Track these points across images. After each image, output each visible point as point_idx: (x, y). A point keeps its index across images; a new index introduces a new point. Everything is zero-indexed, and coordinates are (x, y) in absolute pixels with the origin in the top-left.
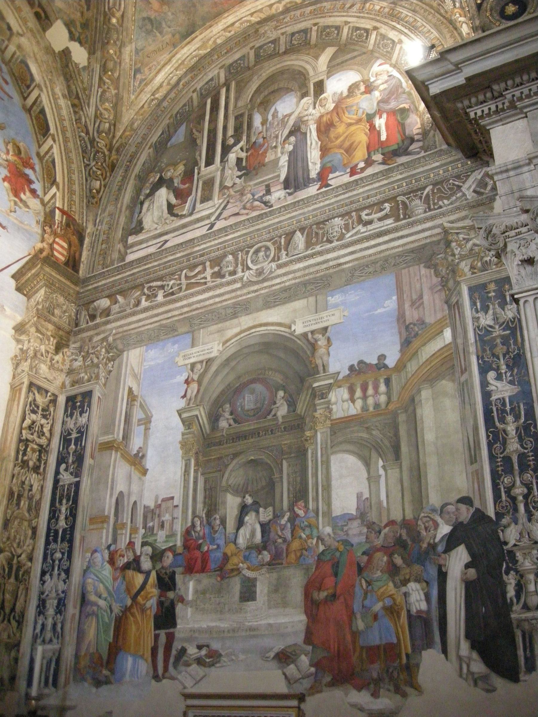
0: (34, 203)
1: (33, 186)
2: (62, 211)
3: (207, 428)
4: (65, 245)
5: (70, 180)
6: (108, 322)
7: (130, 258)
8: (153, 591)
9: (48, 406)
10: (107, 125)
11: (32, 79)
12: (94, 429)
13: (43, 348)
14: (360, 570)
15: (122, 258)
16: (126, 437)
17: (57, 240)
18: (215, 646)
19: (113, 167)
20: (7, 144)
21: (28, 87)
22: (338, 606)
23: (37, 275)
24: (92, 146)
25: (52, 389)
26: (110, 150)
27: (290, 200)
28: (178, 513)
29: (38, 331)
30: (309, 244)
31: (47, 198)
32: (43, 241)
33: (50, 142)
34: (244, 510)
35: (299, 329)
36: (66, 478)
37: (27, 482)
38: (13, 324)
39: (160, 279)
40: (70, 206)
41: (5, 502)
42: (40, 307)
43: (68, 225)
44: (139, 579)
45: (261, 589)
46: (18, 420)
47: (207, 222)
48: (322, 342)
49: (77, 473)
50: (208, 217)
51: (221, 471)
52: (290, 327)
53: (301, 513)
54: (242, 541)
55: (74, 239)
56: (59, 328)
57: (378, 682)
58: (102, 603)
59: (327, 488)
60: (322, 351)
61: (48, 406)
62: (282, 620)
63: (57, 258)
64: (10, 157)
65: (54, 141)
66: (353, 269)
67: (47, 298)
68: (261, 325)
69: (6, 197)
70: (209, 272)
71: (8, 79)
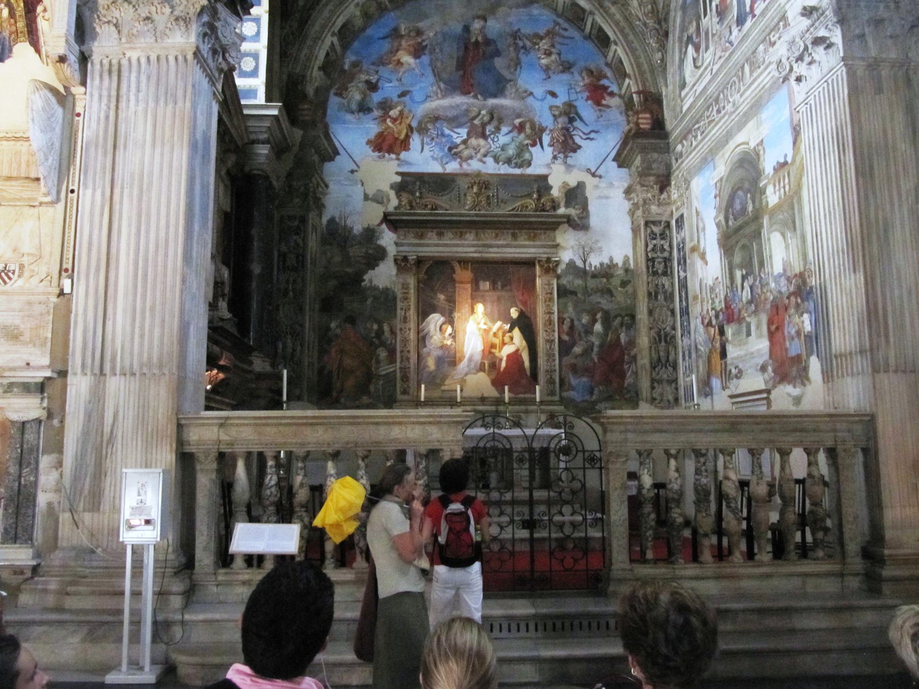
0: (614, 102)
1: (610, 90)
2: (639, 93)
3: (725, 227)
4: (648, 116)
5: (639, 66)
6: (682, 162)
7: (685, 109)
8: (718, 337)
9: (664, 231)
10: (650, 7)
11: (583, 10)
12: (687, 240)
13: (649, 195)
14: (786, 309)
15: (681, 112)
16: (698, 241)
17: (640, 116)
18: (741, 366)
19: (666, 34)
20: (580, 74)
21: (583, 20)
22: (779, 334)
23: (631, 149)
24: (647, 28)
25: (664, 219)
26: (659, 23)
27: (741, 35)
28: (721, 288)
29: (643, 186)
30: (751, 72)
31: (623, 91)
32: (629, 122)
33: (613, 47)
34: (744, 278)
35: (752, 144)
36: (682, 274)
37: (660, 284)
38: (622, 190)
39: (697, 122)
40: (644, 85)
41: (646, 300)
42: (640, 169)
43: (646, 100)
44: (712, 330)
45: (753, 328)
46: (643, 248)
47: (709, 68)
48: (761, 152)
49: (685, 271)
50: (709, 64)
51: (733, 255)
52: (748, 144)
53: (763, 276)
54: (744, 299)
55: (655, 107)
56: (658, 176)
57: (795, 378)
58: (702, 349)
59: (771, 257)
60: (762, 158)
61: (664, 231)
62: (761, 346)
63: (644, 129)
64: (587, 81)
65: (616, 44)
66: (771, 87)
67: (643, 161)
68: (739, 145)
69: (592, 111)
70: (715, 109)
71: (566, 25)
